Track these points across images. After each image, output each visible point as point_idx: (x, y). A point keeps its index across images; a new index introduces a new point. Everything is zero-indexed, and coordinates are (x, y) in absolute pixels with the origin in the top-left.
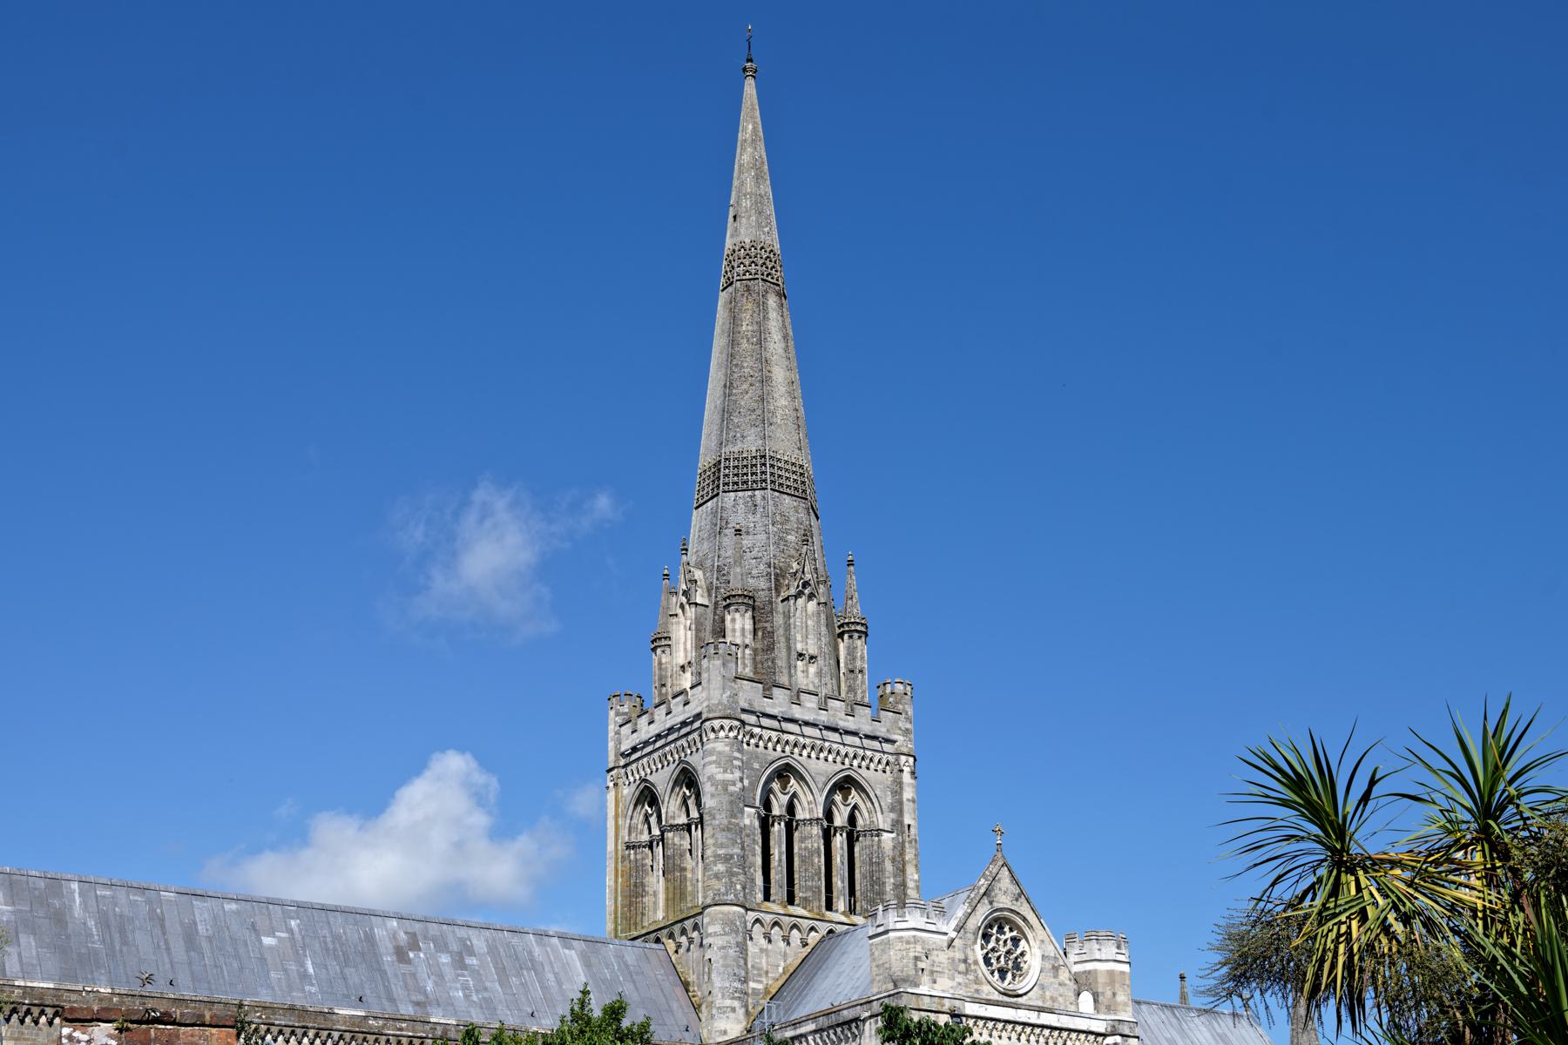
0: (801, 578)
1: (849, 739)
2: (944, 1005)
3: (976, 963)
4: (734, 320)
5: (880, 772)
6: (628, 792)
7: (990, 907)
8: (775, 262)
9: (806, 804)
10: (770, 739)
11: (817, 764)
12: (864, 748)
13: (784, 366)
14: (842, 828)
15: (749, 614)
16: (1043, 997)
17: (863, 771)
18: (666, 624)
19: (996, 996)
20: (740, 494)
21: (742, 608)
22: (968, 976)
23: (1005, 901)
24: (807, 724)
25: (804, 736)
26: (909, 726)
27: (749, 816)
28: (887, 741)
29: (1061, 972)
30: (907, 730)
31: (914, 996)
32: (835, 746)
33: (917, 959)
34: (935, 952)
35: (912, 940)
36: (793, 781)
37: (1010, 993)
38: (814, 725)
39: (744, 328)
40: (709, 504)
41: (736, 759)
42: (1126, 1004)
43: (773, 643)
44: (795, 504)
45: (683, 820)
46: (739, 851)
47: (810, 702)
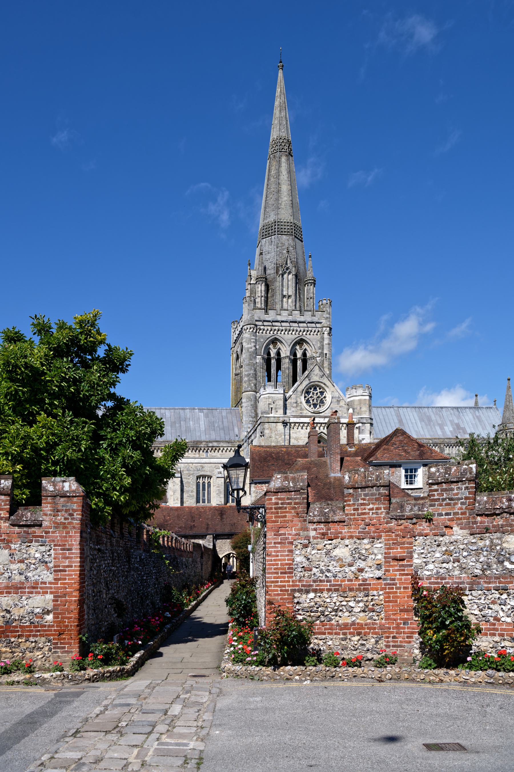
0: (285, 267)
1: (301, 325)
3: (301, 403)
5: (315, 335)
9: (284, 351)
10: (268, 330)
12: (308, 327)
14: (299, 358)
17: (308, 336)
21: (261, 282)
24: (283, 322)
25: (282, 326)
26: (328, 316)
32: (295, 328)
33: (269, 404)
36: (278, 343)
38: (286, 322)
41: (252, 339)
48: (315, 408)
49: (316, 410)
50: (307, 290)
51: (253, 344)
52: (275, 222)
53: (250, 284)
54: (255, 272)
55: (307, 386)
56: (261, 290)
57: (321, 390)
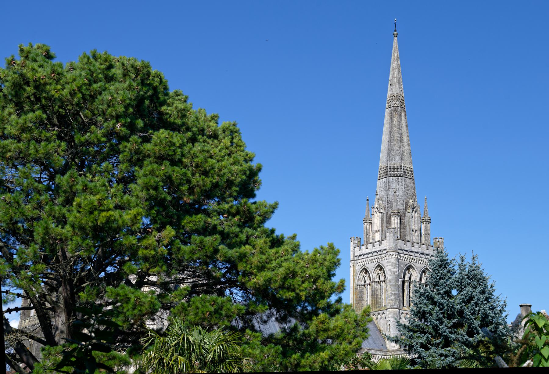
4: (392, 120)
6: (358, 268)
15: (399, 218)
18: (371, 217)
24: (416, 252)
36: (411, 270)
39: (395, 123)
40: (384, 179)
43: (405, 226)
45: (377, 280)
47: (417, 246)
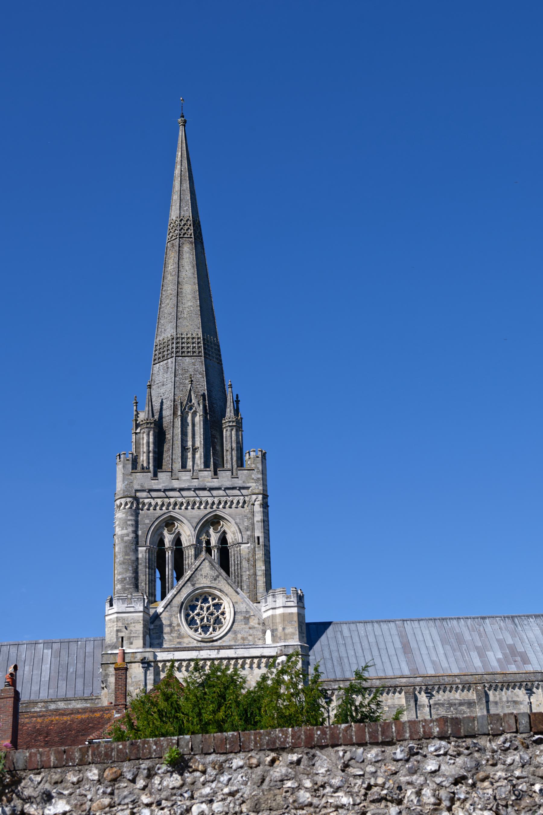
0: (187, 404)
2: (136, 657)
5: (240, 508)
7: (192, 588)
8: (190, 225)
11: (192, 512)
13: (192, 283)
16: (235, 639)
19: (195, 644)
20: (161, 363)
22: (172, 635)
23: (205, 582)
24: (181, 490)
27: (141, 552)
28: (244, 488)
29: (251, 620)
30: (258, 478)
31: (112, 655)
34: (133, 625)
35: (115, 620)
37: (206, 640)
39: (169, 268)
41: (131, 520)
42: (293, 634)
44: (193, 361)
46: (131, 575)
48: (206, 633)
49: (207, 635)
50: (226, 437)
51: (131, 529)
52: (173, 339)
53: (136, 433)
54: (144, 414)
55: (189, 595)
56: (148, 443)
57: (216, 601)
